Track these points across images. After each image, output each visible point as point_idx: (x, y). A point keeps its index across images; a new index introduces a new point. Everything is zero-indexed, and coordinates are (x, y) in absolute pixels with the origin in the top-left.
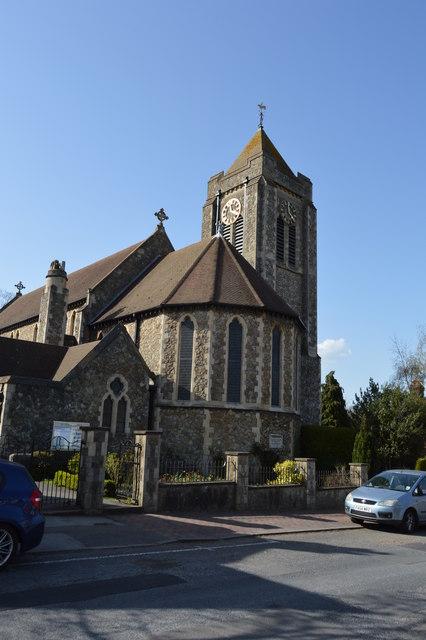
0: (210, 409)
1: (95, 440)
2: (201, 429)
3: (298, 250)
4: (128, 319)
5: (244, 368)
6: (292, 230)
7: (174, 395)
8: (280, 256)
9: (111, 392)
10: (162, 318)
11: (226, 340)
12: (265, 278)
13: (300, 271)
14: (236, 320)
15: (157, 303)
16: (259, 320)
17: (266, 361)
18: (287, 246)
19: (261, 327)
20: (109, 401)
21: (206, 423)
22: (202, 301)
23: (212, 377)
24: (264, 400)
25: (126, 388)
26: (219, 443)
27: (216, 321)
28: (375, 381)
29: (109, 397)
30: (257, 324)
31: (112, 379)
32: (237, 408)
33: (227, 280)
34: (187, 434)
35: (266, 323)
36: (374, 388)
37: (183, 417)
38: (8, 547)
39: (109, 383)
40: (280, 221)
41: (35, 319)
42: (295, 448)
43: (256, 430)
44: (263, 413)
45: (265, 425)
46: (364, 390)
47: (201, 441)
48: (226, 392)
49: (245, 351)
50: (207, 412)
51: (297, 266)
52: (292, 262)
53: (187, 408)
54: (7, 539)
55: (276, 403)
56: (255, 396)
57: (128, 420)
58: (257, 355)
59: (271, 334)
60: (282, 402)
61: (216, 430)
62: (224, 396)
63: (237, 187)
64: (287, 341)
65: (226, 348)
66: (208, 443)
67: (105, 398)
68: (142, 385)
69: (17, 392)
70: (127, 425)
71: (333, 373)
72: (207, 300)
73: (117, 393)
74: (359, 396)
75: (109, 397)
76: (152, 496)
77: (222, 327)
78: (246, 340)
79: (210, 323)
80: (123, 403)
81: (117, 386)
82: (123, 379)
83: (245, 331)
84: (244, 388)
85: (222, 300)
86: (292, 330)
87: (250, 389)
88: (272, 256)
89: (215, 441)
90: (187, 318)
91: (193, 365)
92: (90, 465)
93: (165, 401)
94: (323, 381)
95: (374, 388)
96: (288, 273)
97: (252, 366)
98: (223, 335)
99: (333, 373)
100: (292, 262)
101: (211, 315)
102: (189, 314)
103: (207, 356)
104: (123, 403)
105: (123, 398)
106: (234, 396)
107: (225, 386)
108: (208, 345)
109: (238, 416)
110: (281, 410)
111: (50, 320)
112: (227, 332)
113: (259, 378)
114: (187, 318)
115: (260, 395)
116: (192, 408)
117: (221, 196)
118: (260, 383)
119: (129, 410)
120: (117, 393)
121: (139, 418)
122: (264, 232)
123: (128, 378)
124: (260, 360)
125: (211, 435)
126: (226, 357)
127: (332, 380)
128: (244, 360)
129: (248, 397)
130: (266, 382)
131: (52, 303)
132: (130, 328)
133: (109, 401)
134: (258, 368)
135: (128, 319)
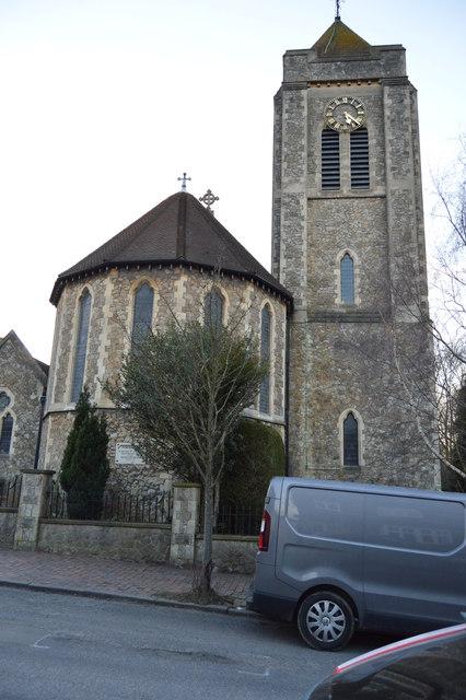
6: (359, 134)
8: (331, 180)
13: (379, 191)
18: (345, 161)
25: (12, 403)
30: (104, 287)
52: (360, 181)
59: (131, 297)
68: (33, 397)
96: (348, 202)
98: (71, 315)
100: (360, 181)
113: (100, 363)
119: (15, 427)
121: (27, 436)
134: (101, 349)
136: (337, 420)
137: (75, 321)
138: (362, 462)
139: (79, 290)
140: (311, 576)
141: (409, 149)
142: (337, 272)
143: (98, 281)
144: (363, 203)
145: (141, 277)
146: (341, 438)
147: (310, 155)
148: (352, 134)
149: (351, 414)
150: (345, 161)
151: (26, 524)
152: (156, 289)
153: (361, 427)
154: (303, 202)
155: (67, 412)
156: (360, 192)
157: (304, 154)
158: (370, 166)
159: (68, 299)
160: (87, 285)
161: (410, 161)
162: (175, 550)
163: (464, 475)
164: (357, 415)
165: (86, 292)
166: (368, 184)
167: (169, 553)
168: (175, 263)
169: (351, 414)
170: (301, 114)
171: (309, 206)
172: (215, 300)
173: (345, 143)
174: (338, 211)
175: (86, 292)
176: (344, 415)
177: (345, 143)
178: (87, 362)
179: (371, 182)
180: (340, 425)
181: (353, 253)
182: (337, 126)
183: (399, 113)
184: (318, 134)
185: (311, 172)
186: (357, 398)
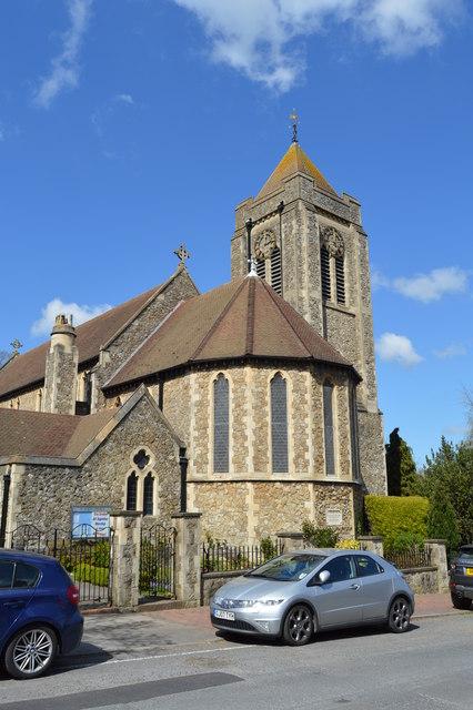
1: (128, 527)
2: (243, 507)
3: (346, 285)
4: (150, 379)
5: (290, 431)
6: (339, 265)
7: (210, 467)
8: (326, 295)
9: (135, 467)
10: (193, 378)
11: (268, 399)
12: (307, 318)
13: (352, 310)
14: (278, 375)
15: (183, 360)
16: (307, 374)
18: (333, 281)
20: (132, 480)
21: (249, 499)
22: (237, 355)
23: (254, 444)
24: (317, 469)
25: (151, 462)
26: (266, 522)
27: (255, 378)
28: (448, 440)
29: (134, 473)
31: (136, 452)
33: (261, 327)
34: (226, 513)
35: (314, 376)
36: (446, 448)
37: (221, 493)
38: (47, 649)
39: (132, 457)
40: (324, 253)
41: (39, 383)
42: (356, 524)
43: (310, 505)
44: (316, 483)
45: (321, 498)
46: (436, 450)
47: (243, 524)
48: (270, 461)
49: (290, 411)
50: (249, 484)
51: (347, 303)
53: (226, 482)
54: (45, 640)
55: (331, 471)
57: (156, 500)
60: (338, 469)
61: (262, 506)
62: (269, 467)
63: (271, 214)
64: (340, 396)
65: (268, 409)
66: (252, 523)
67: (129, 474)
68: (171, 458)
69: (26, 474)
70: (155, 506)
71: (397, 430)
72: (241, 353)
73: (141, 468)
74: (430, 458)
75: (134, 473)
76: (193, 587)
77: (259, 383)
78: (291, 397)
79: (248, 380)
80: (149, 481)
81: (141, 459)
82: (148, 452)
83: (290, 386)
84: (291, 455)
85: (255, 353)
86: (346, 383)
87: (298, 456)
88: (318, 295)
89: (262, 521)
90: (221, 375)
91: (231, 431)
92: (119, 555)
93: (199, 476)
94: (387, 441)
95: (446, 448)
97: (301, 429)
99: (397, 430)
100: (341, 299)
101: (248, 371)
102: (223, 371)
103: (249, 422)
104: (149, 481)
105: (150, 474)
106: (280, 464)
107: (269, 454)
108: (248, 406)
109: (287, 488)
110: (337, 478)
111: (59, 387)
112: (268, 389)
113: (309, 443)
114: (221, 375)
115: (312, 463)
116: (232, 482)
117: (250, 226)
118: (311, 449)
120: (141, 468)
121: (170, 497)
122: (305, 267)
123: (156, 450)
124: (308, 421)
125: (256, 513)
126: (269, 419)
127: (394, 436)
128: (290, 421)
129: (297, 466)
130: (316, 443)
131: (60, 365)
132: (153, 390)
133: (132, 480)
134: (309, 431)
135: (150, 379)
150: (333, 281)
154: (321, 307)
173: (332, 262)
177: (332, 262)
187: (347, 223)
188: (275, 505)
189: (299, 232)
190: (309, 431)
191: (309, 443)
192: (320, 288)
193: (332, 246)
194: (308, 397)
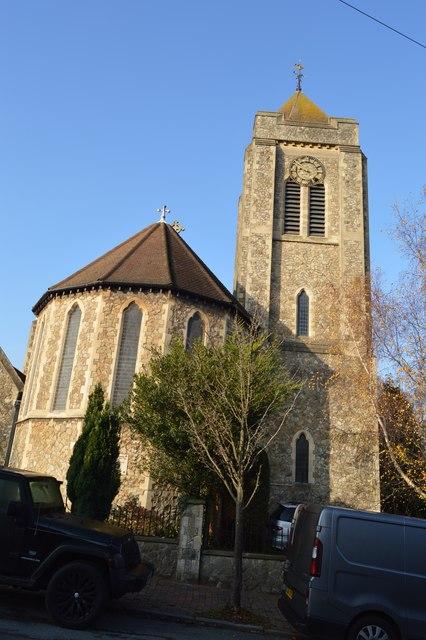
0: (33, 419)
6: (316, 189)
13: (334, 239)
17: (103, 351)
18: (304, 212)
19: (98, 310)
32: (58, 416)
51: (326, 234)
56: (79, 402)
58: (90, 345)
88: (266, 230)
96: (307, 246)
98: (59, 327)
100: (316, 227)
113: (87, 374)
124: (91, 351)
134: (89, 362)
136: (291, 439)
137: (62, 332)
138: (312, 480)
139: (68, 303)
140: (360, 601)
141: (361, 207)
142: (295, 306)
143: (89, 298)
144: (319, 248)
145: (130, 297)
146: (293, 457)
147: (276, 202)
148: (311, 188)
149: (303, 435)
150: (304, 212)
151: (190, 555)
152: (145, 312)
153: (312, 447)
154: (269, 242)
155: (50, 419)
156: (315, 238)
157: (272, 201)
158: (326, 216)
159: (57, 312)
160: (77, 300)
161: (361, 218)
162: (181, 563)
163: (423, 496)
164: (309, 437)
165: (75, 307)
166: (323, 233)
167: (175, 568)
168: (165, 289)
169: (303, 435)
170: (270, 167)
171: (273, 246)
172: (195, 325)
173: (304, 192)
174: (298, 253)
175: (75, 307)
176: (297, 436)
177: (304, 192)
178: (73, 373)
179: (326, 230)
180: (293, 445)
181: (308, 292)
182: (299, 180)
183: (353, 176)
184: (282, 185)
185: (276, 216)
186: (310, 421)
187: (332, 146)
188: (45, 445)
189: (250, 169)
190: (89, 362)
191: (87, 374)
192: (270, 222)
193: (304, 176)
194: (96, 324)
